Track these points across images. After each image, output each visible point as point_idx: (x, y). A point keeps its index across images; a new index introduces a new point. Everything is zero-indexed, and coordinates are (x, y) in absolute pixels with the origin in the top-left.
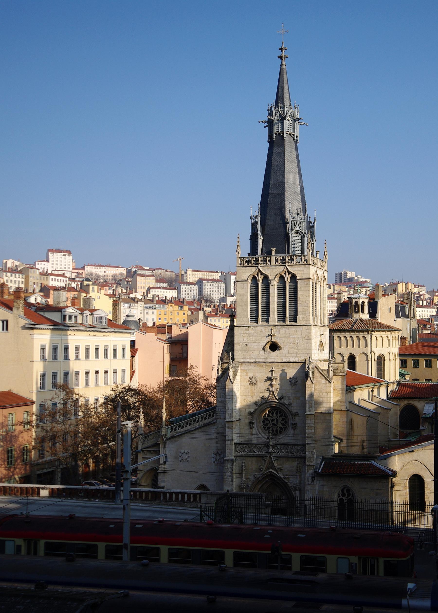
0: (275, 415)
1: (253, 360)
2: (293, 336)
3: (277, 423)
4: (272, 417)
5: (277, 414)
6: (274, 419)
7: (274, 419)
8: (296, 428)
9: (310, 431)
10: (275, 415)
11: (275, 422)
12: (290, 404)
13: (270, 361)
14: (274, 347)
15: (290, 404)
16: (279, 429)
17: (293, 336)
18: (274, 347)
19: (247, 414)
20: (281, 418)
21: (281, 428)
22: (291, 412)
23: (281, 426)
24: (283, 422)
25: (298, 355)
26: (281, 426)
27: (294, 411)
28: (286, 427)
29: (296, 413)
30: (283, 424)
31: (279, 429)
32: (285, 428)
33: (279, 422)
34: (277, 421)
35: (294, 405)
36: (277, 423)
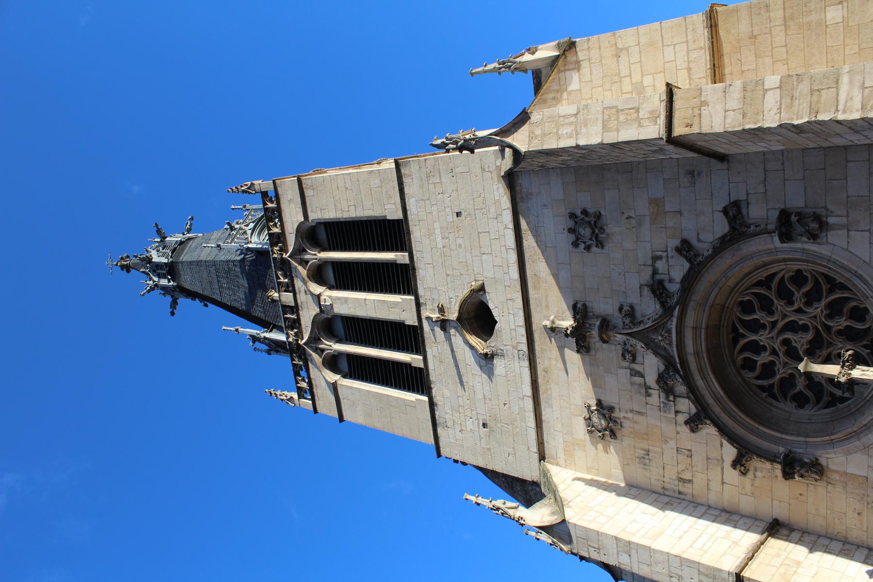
0: (762, 337)
1: (529, 404)
2: (438, 231)
3: (805, 328)
4: (774, 352)
5: (756, 327)
7: (786, 342)
8: (817, 218)
9: (771, 100)
10: (762, 337)
11: (800, 341)
12: (685, 248)
13: (523, 331)
14: (478, 317)
15: (685, 248)
17: (438, 231)
18: (478, 317)
19: (747, 480)
20: (779, 304)
22: (724, 244)
23: (819, 309)
25: (492, 210)
27: (722, 227)
29: (725, 211)
30: (811, 298)
32: (834, 285)
33: (802, 319)
34: (792, 327)
35: (688, 227)
36: (805, 328)
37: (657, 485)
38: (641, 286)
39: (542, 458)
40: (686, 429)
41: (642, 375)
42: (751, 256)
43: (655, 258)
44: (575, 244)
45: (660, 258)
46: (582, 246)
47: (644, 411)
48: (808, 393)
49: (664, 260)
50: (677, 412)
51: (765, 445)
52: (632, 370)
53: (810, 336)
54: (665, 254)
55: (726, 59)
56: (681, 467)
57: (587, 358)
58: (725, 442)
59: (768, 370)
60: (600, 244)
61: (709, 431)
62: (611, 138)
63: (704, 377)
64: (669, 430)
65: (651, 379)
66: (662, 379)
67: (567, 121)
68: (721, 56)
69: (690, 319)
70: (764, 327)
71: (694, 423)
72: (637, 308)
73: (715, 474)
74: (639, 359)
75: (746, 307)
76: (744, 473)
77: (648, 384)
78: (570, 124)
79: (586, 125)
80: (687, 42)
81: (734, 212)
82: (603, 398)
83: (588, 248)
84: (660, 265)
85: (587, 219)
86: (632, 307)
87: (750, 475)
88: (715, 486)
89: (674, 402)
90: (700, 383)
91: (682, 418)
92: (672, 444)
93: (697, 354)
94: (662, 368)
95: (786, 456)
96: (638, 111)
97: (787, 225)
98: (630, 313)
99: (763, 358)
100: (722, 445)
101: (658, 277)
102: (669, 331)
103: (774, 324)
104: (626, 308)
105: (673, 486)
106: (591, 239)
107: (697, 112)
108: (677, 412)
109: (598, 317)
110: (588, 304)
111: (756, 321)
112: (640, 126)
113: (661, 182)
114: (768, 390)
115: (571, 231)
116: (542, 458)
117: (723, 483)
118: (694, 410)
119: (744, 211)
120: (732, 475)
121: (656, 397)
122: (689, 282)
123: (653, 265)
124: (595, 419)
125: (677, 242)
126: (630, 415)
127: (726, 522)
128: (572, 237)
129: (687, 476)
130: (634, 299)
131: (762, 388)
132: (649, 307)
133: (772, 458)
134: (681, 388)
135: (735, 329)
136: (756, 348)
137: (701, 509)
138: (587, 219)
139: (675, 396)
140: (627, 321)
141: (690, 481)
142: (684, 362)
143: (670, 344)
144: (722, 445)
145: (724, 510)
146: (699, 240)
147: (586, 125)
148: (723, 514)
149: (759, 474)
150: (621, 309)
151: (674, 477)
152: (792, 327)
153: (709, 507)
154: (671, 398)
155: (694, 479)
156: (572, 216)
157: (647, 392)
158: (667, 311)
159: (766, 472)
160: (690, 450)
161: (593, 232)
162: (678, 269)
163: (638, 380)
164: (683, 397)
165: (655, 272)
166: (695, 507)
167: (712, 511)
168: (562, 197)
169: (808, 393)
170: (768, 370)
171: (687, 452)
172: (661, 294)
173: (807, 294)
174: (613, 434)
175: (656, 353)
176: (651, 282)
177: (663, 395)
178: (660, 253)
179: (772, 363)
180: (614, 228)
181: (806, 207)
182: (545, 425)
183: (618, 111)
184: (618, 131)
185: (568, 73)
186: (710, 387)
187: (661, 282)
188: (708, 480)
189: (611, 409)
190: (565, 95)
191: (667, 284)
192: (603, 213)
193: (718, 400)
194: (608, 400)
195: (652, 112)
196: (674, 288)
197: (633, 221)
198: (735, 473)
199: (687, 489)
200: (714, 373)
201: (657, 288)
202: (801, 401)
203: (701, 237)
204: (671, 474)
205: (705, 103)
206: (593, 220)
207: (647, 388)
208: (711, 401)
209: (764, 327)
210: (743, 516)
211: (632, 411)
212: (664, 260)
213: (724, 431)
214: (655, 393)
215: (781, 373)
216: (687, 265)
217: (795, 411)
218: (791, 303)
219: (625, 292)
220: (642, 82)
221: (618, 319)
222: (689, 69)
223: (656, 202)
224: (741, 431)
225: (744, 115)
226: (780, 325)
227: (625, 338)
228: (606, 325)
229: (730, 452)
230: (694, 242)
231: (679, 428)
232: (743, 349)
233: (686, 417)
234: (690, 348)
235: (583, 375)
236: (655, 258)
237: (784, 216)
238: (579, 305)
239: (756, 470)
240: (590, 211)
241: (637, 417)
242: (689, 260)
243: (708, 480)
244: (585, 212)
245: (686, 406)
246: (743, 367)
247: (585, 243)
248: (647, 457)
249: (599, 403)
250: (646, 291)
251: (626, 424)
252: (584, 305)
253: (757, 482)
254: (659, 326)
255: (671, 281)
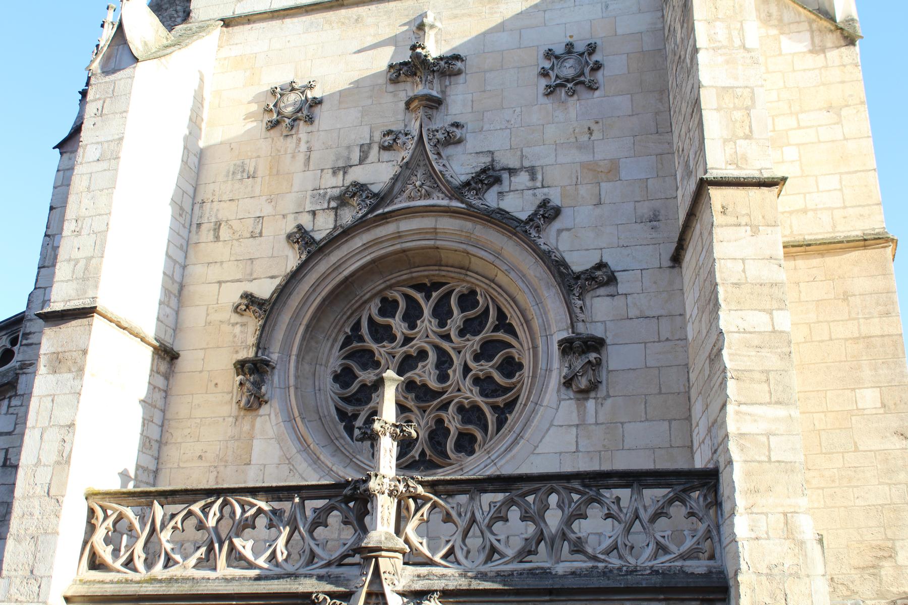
0: (427, 323)
3: (443, 377)
4: (407, 340)
5: (442, 313)
6: (422, 355)
7: (422, 355)
9: (758, 321)
10: (427, 323)
11: (426, 373)
12: (548, 213)
15: (548, 213)
16: (453, 423)
19: (228, 314)
20: (474, 342)
21: (471, 413)
23: (471, 394)
24: (487, 367)
26: (471, 394)
27: (579, 262)
28: (511, 405)
29: (601, 266)
30: (484, 384)
31: (453, 423)
32: (503, 413)
34: (444, 361)
36: (443, 377)
37: (205, 193)
38: (492, 153)
39: (227, 23)
40: (290, 227)
41: (362, 161)
42: (539, 303)
43: (532, 172)
44: (549, 54)
45: (533, 178)
46: (547, 65)
47: (311, 167)
48: (355, 387)
49: (530, 184)
50: (314, 213)
51: (279, 335)
52: (369, 145)
53: (433, 384)
54: (539, 184)
55: (816, 261)
56: (235, 224)
57: (382, 80)
58: (277, 282)
59: (383, 333)
60: (550, 91)
61: (292, 259)
62: (707, 100)
63: (366, 247)
64: (288, 204)
65: (358, 174)
66: (359, 188)
67: (735, 33)
68: (822, 254)
69: (447, 224)
70: (442, 324)
71: (300, 237)
72: (459, 148)
73: (231, 271)
74: (386, 155)
75: (468, 300)
76: (236, 310)
77: (351, 171)
78: (730, 39)
79: (727, 62)
80: (845, 207)
81: (601, 277)
82: (325, 106)
83: (544, 74)
84: (523, 179)
85: (587, 70)
86: (460, 141)
87: (236, 318)
88: (215, 273)
89: (328, 208)
90: (358, 242)
91: (306, 221)
92: (268, 210)
93: (399, 236)
94: (375, 189)
95: (267, 363)
96: (747, 137)
97: (584, 348)
98: (450, 139)
99: (398, 325)
100: (272, 277)
101: (505, 176)
102: (428, 195)
103: (447, 337)
104: (458, 133)
105: (207, 215)
106: (557, 77)
107: (743, 220)
108: (314, 213)
109: (443, 92)
110: (461, 78)
111: (450, 314)
112: (725, 141)
113: (643, 176)
114: (355, 334)
115: (570, 47)
116: (227, 23)
117: (220, 282)
118: (318, 236)
119: (602, 291)
120: (233, 295)
121: (334, 183)
122: (500, 219)
123: (522, 168)
124: (293, 98)
125: (556, 201)
126: (303, 147)
127: (166, 291)
128: (559, 50)
129: (224, 233)
130: (472, 143)
131: (357, 327)
132: (461, 165)
133: (261, 345)
134: (348, 216)
135: (437, 286)
136: (412, 316)
137: (179, 256)
138: (587, 70)
139: (336, 209)
140: (440, 136)
141: (217, 238)
142: (385, 218)
143: (410, 198)
144: (272, 277)
145: (182, 287)
146: (559, 231)
147: (727, 62)
148: (176, 286)
149: (238, 329)
150: (456, 125)
151: (220, 217)
152: (444, 361)
153: (184, 267)
154: (333, 204)
155: (220, 243)
156: (592, 49)
157: (339, 169)
158: (458, 192)
159: (242, 337)
160: (261, 235)
161: (568, 81)
162: (517, 202)
163: (356, 156)
164: (336, 221)
165: (512, 171)
166: (181, 248)
167: (178, 270)
168: (620, 31)
169: (355, 387)
170: (383, 333)
171: (258, 231)
172: (481, 181)
173: (489, 378)
174: (274, 125)
175: (396, 179)
176: (498, 167)
177: (337, 192)
178: (539, 177)
179: (393, 338)
180: (575, 110)
181: (609, 372)
182: (276, 23)
183: (747, 108)
184: (718, 109)
185: (808, 35)
186: (352, 256)
187: (498, 180)
188: (222, 263)
189: (310, 120)
190: (774, 32)
191: (495, 189)
192: (597, 93)
193: (336, 267)
194: (323, 115)
195: (745, 158)
196: (491, 199)
197: (585, 138)
198: (236, 299)
199: (206, 234)
200: (373, 261)
201: (488, 177)
202: (344, 377)
203: (565, 234)
204: (225, 211)
205: (755, 230)
206: (586, 78)
207: (345, 169)
208: (335, 257)
209: (442, 324)
210: (177, 313)
211: (310, 150)
212: (530, 184)
213: (294, 277)
214: (338, 181)
215: (380, 350)
216: (524, 216)
217: (329, 371)
218: (477, 358)
219: (481, 130)
220: (789, 144)
221: (441, 121)
222: (805, 211)
223: (613, 170)
224: (295, 300)
225: (737, 285)
226: (446, 345)
227: (416, 133)
228: (433, 104)
229: (264, 289)
230: (557, 225)
231: (291, 217)
232: (407, 297)
233: (308, 226)
234: (406, 225)
235: (356, 76)
236: (532, 172)
237: (596, 344)
238: (459, 64)
239: (243, 325)
240: (599, 75)
241: (301, 158)
242: (531, 219)
243: (222, 263)
244: (597, 67)
245: (323, 227)
246: (384, 300)
247: (552, 68)
248: (245, 175)
249: (317, 102)
250: (485, 161)
251: (291, 143)
252: (459, 72)
253: (226, 328)
254: (436, 180)
255: (501, 194)
